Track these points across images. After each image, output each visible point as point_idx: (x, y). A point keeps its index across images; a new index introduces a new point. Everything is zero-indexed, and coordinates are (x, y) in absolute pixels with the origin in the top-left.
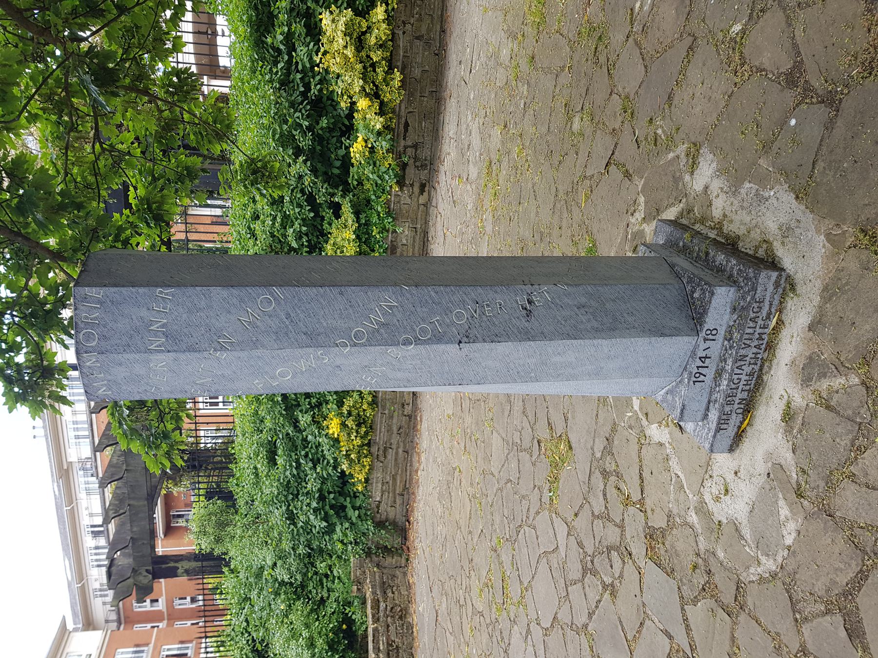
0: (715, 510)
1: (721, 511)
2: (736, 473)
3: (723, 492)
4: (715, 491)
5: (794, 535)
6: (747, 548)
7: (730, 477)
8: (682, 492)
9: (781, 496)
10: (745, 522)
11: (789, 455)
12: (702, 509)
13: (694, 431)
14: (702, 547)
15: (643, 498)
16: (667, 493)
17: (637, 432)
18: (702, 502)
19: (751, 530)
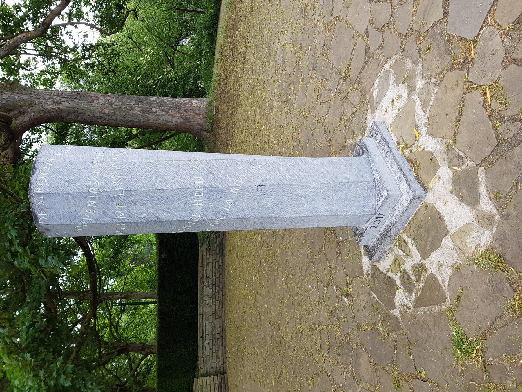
0: (403, 90)
1: (402, 90)
2: (386, 111)
3: (395, 101)
4: (399, 101)
5: (375, 83)
6: (393, 72)
7: (390, 109)
8: (423, 100)
9: (374, 100)
10: (390, 86)
11: (368, 117)
12: (411, 89)
13: (377, 134)
14: (420, 65)
15: (465, 93)
16: (436, 99)
17: (453, 151)
18: (409, 94)
19: (389, 82)
